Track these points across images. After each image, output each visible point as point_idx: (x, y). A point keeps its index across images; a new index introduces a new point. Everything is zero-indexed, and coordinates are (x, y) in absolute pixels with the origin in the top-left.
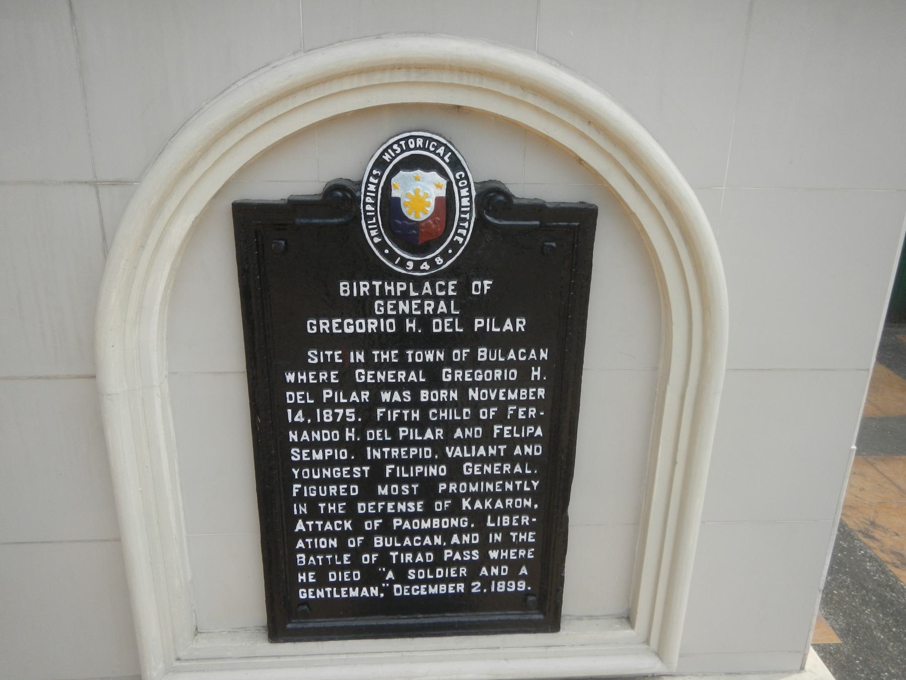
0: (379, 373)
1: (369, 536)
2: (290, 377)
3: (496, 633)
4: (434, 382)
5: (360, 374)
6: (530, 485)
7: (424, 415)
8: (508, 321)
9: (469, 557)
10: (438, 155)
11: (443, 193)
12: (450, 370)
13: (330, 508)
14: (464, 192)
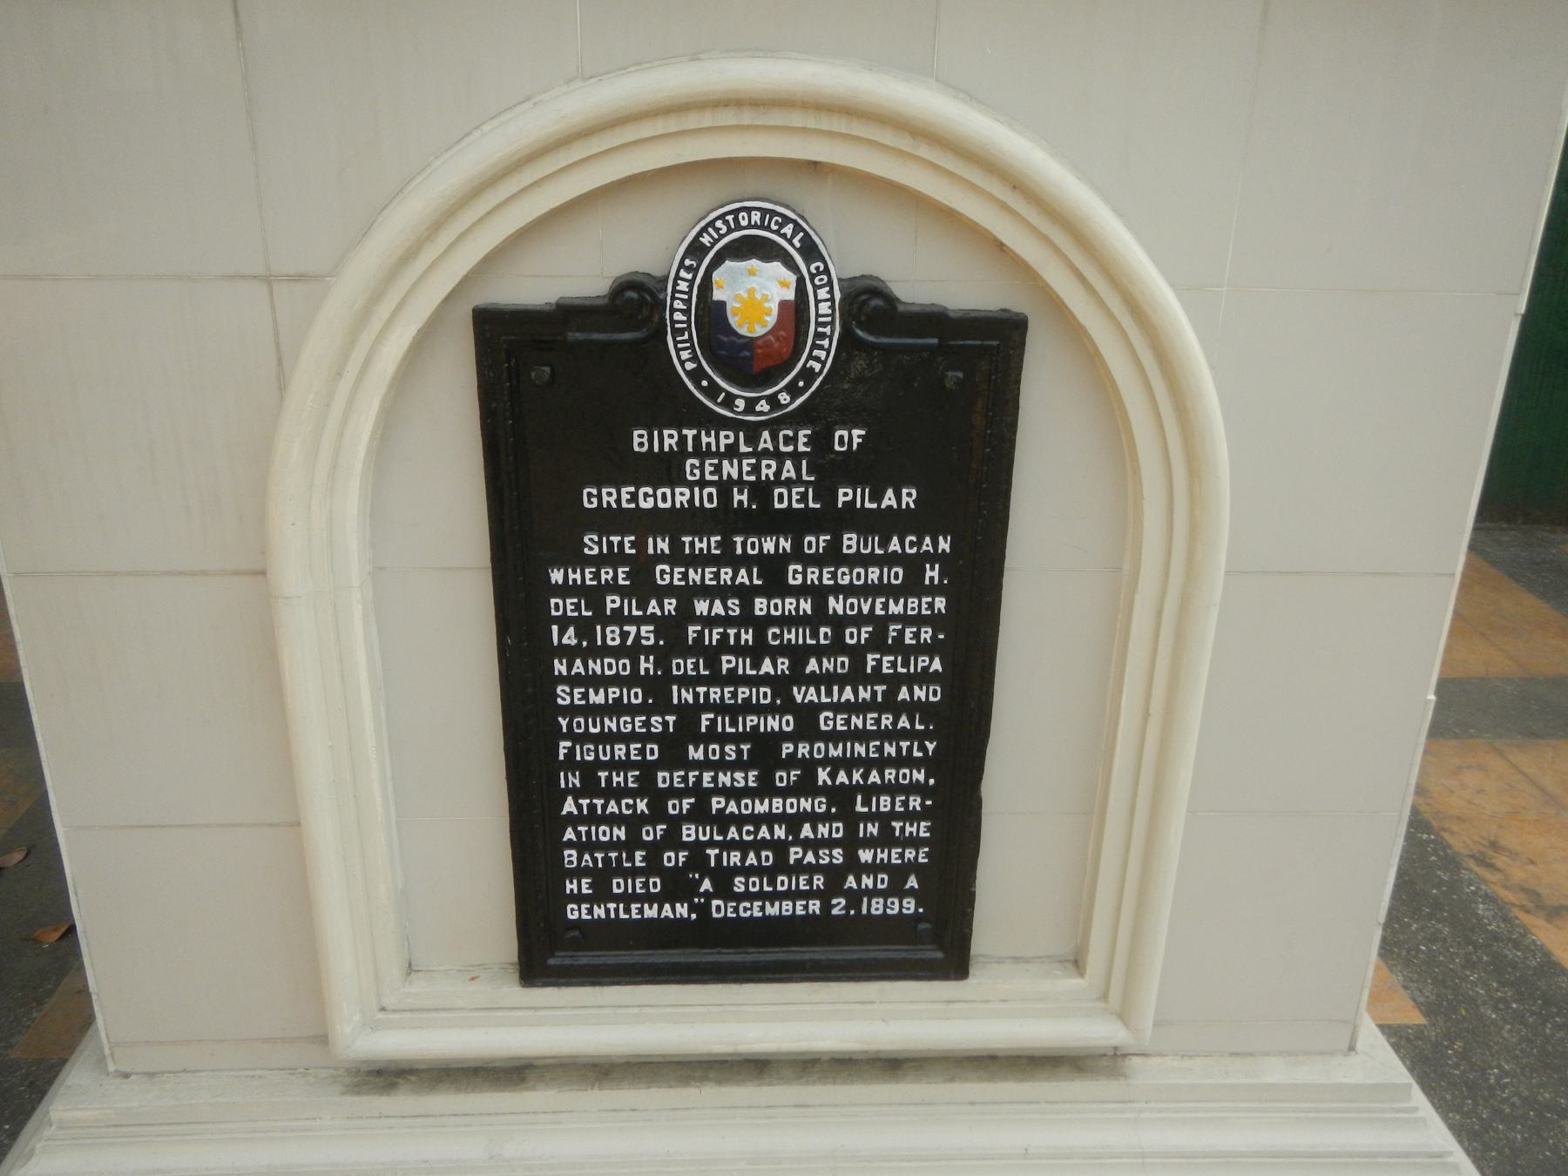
0: (691, 571)
1: (675, 823)
2: (557, 576)
3: (868, 979)
4: (775, 585)
5: (663, 572)
6: (922, 748)
7: (760, 636)
8: (890, 493)
9: (827, 860)
10: (784, 236)
11: (790, 295)
12: (800, 568)
13: (615, 779)
14: (823, 293)
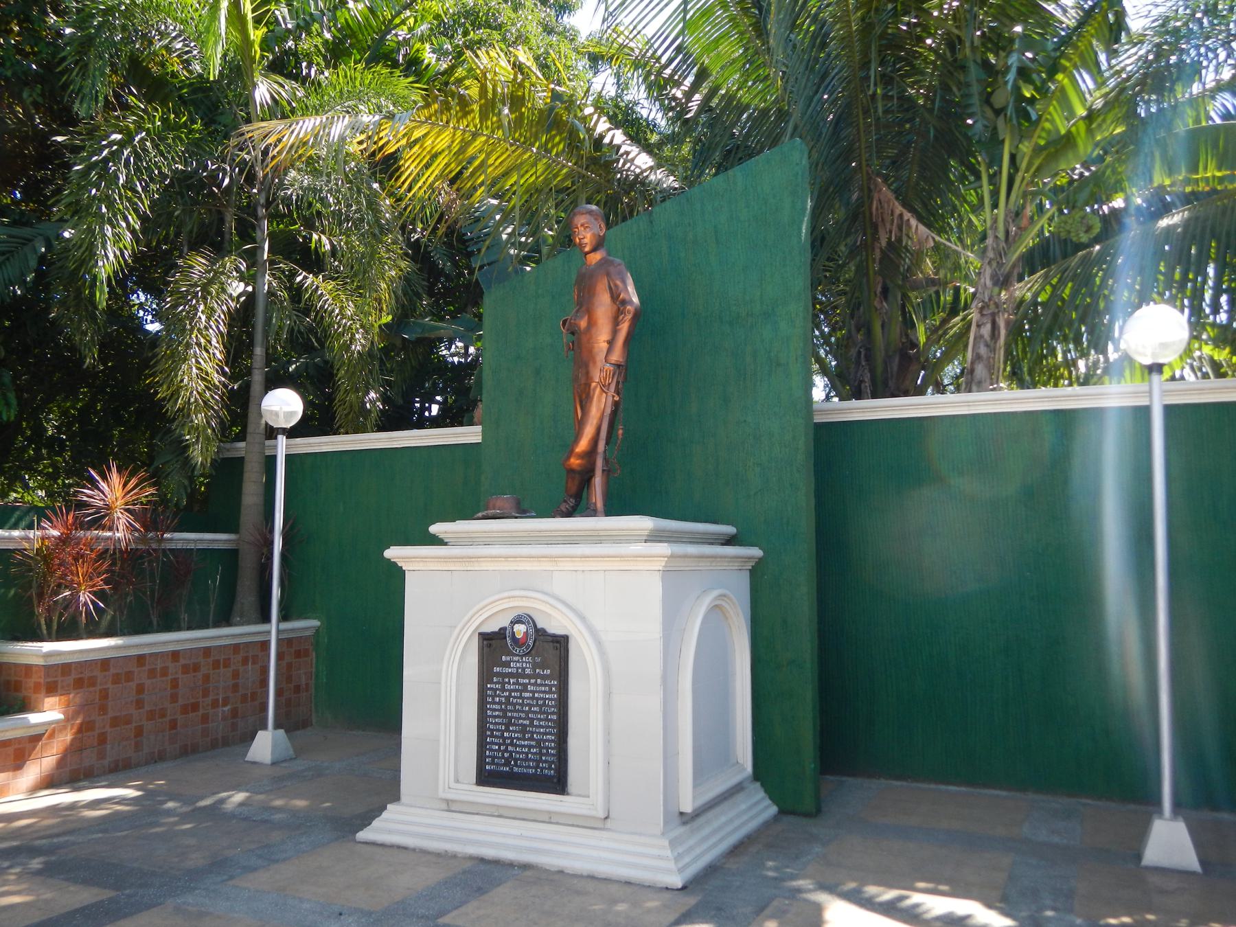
1: (507, 746)
